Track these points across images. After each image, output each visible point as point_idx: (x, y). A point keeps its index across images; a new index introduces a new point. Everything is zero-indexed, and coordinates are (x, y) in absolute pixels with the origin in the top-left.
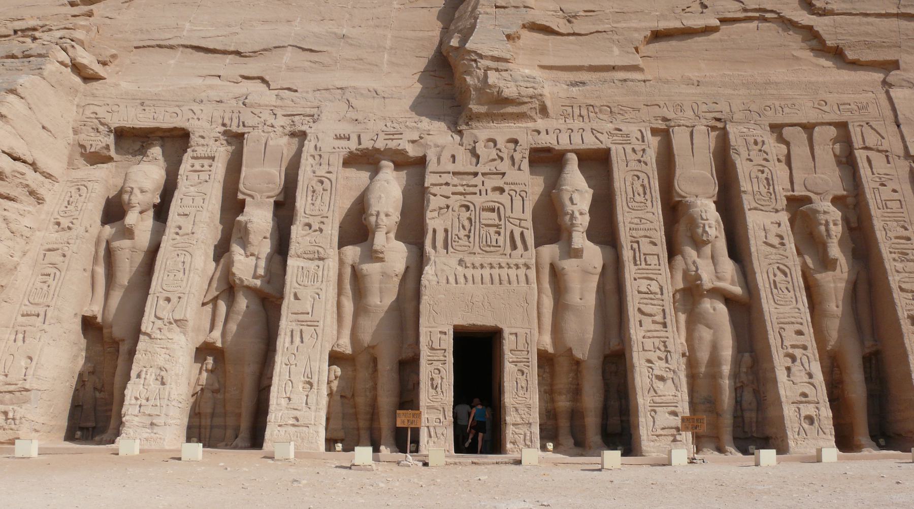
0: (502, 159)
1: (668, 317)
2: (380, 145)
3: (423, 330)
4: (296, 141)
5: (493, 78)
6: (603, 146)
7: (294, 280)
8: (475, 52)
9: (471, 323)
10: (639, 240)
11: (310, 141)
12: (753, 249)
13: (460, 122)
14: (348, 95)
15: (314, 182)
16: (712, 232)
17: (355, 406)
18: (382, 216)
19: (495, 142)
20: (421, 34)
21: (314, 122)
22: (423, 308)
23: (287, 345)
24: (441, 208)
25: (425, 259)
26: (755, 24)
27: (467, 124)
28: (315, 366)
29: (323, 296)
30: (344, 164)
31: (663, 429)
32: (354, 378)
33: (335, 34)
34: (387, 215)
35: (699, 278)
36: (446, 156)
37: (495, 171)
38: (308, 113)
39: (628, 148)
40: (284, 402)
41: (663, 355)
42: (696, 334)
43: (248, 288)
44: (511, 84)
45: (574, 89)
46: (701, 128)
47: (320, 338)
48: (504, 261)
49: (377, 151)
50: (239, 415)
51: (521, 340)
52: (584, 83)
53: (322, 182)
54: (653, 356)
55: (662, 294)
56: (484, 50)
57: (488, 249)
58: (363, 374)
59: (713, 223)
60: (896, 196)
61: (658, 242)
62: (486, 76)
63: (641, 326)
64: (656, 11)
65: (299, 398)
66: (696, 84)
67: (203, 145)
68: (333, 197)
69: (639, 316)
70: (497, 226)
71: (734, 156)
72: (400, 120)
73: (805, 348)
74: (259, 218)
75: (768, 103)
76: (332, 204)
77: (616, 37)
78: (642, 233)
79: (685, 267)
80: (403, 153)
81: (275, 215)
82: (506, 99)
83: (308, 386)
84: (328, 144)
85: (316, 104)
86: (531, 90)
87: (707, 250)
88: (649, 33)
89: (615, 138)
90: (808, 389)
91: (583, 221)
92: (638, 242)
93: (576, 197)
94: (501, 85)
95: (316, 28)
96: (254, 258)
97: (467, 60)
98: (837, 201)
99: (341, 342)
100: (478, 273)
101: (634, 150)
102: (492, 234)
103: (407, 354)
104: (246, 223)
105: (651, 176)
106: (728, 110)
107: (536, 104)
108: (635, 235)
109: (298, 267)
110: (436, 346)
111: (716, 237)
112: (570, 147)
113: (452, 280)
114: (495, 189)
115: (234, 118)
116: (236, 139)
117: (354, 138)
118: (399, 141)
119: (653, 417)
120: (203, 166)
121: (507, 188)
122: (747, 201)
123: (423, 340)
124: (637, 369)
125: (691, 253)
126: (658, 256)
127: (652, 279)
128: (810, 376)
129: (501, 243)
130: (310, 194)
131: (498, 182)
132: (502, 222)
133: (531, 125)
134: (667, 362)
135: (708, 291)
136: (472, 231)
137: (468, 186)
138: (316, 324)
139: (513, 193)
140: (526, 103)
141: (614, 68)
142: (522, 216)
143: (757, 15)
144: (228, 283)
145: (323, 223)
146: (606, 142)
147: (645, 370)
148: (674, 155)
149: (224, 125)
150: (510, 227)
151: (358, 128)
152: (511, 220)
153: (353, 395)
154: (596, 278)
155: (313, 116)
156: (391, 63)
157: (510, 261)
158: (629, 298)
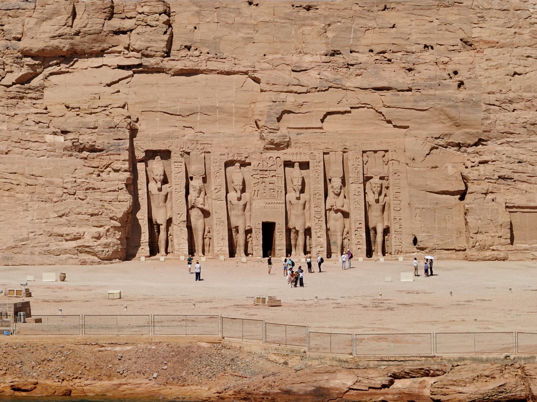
2: (235, 159)
6: (307, 161)
43: (198, 208)
49: (235, 160)
54: (317, 231)
75: (363, 142)
80: (244, 161)
82: (276, 144)
85: (212, 139)
88: (325, 113)
121: (277, 175)
131: (273, 173)
133: (285, 151)
140: (283, 145)
141: (313, 128)
143: (364, 105)
156: (236, 121)
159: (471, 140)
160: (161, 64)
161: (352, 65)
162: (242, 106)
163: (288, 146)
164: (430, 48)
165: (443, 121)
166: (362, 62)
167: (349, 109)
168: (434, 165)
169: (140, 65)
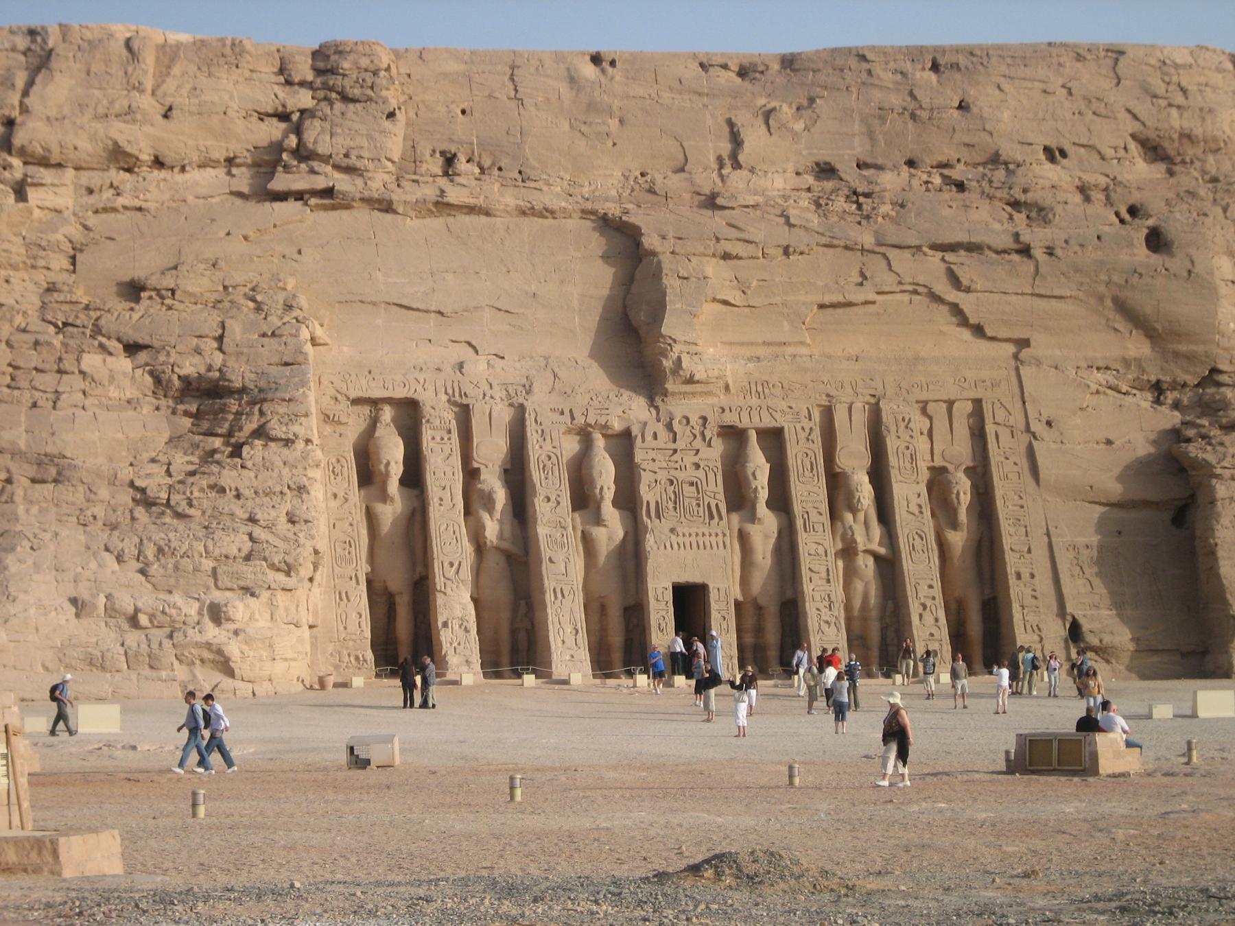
6: (777, 425)
12: (897, 517)
13: (657, 399)
35: (855, 542)
39: (799, 427)
40: (560, 644)
43: (497, 548)
44: (701, 367)
45: (751, 365)
46: (858, 405)
49: (590, 425)
53: (550, 458)
54: (821, 606)
59: (867, 495)
60: (1016, 468)
61: (823, 511)
62: (679, 359)
65: (570, 641)
69: (809, 573)
71: (885, 433)
73: (934, 598)
77: (786, 311)
84: (548, 418)
87: (861, 516)
90: (934, 630)
91: (763, 494)
93: (758, 474)
98: (969, 471)
101: (803, 428)
107: (721, 384)
110: (660, 598)
112: (749, 425)
122: (894, 473)
125: (849, 517)
128: (937, 620)
129: (701, 513)
133: (714, 400)
142: (716, 490)
143: (910, 288)
149: (446, 393)
159: (1187, 372)
161: (867, 195)
164: (1057, 154)
165: (1117, 326)
167: (872, 296)
168: (1102, 436)
169: (328, 192)
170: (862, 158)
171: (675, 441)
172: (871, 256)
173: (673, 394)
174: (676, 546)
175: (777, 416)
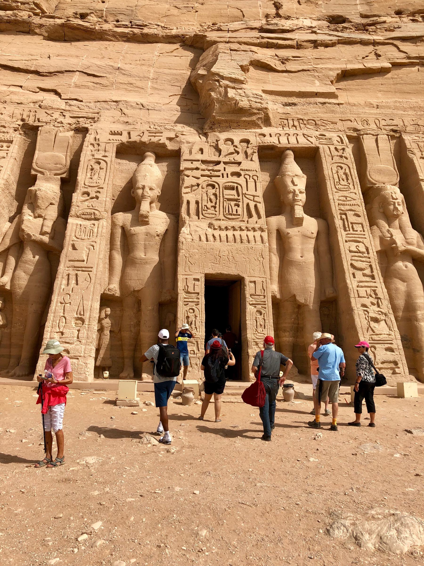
0: (238, 153)
1: (375, 271)
2: (145, 139)
3: (180, 277)
4: (80, 136)
5: (231, 93)
6: (313, 146)
7: (73, 235)
8: (218, 75)
9: (219, 272)
10: (347, 212)
11: (91, 134)
13: (206, 127)
14: (121, 106)
15: (92, 163)
16: (400, 208)
17: (121, 340)
18: (147, 189)
19: (232, 141)
20: (175, 72)
21: (94, 122)
22: (180, 259)
23: (63, 287)
24: (192, 186)
25: (180, 223)
26: (417, 68)
27: (211, 128)
28: (88, 304)
29: (97, 247)
30: (116, 153)
31: (383, 363)
32: (121, 317)
33: (112, 66)
34: (151, 189)
36: (196, 149)
37: (233, 161)
38: (90, 116)
39: (332, 148)
40: (57, 336)
41: (375, 301)
42: (393, 286)
45: (288, 107)
47: (93, 281)
48: (243, 225)
49: (143, 144)
50: (21, 346)
51: (259, 287)
52: (294, 104)
53: (99, 163)
54: (367, 301)
55: (368, 253)
56: (225, 72)
57: (230, 217)
58: (129, 313)
59: (400, 200)
61: (361, 214)
62: (226, 92)
63: (354, 277)
64: (344, 58)
65: (71, 332)
66: (375, 106)
67: (4, 132)
68: (108, 174)
69: (352, 270)
70: (236, 200)
71: (411, 156)
72: (161, 124)
74: (48, 189)
76: (107, 179)
77: (316, 74)
78: (348, 207)
79: (380, 234)
80: (164, 146)
81: (62, 188)
83: (79, 322)
84: (104, 137)
85: (96, 111)
86: (259, 104)
87: (397, 222)
89: (321, 140)
91: (302, 197)
92: (345, 214)
93: (296, 180)
94: (238, 99)
95: (99, 63)
96: (41, 219)
97: (213, 80)
99: (111, 286)
100: (223, 234)
101: (336, 148)
102: (233, 206)
103: (166, 297)
104: (36, 191)
105: (351, 166)
106: (402, 124)
107: (262, 116)
108: (343, 209)
109: (77, 225)
110: (191, 290)
111: (403, 213)
112: (289, 146)
113: (203, 238)
114: (234, 174)
115: (31, 116)
116: (31, 131)
117: (125, 134)
118: (160, 138)
119: (374, 353)
120: (2, 147)
121: (242, 173)
123: (181, 285)
124: (356, 312)
125: (383, 223)
126: (362, 224)
127: (359, 242)
129: (240, 212)
130: (89, 170)
131: (236, 169)
132: (240, 197)
133: (259, 131)
134: (379, 306)
135: (401, 253)
136: (218, 203)
137: (213, 170)
138: (90, 269)
139: (247, 177)
140: (255, 114)
141: (316, 95)
144: (19, 238)
145: (99, 192)
146: (315, 142)
147: (362, 313)
148: (365, 155)
149: (23, 120)
150: (246, 201)
151: (129, 128)
152: (247, 196)
153: (120, 330)
154: (313, 241)
155: (94, 118)
157: (248, 225)
158: (343, 256)
160: (26, 17)
161: (370, 25)
162: (167, 71)
163: (267, 122)
166: (387, 22)
170: (364, 13)
171: (219, 157)
172: (380, 47)
173: (220, 122)
174: (211, 238)
175: (313, 140)
